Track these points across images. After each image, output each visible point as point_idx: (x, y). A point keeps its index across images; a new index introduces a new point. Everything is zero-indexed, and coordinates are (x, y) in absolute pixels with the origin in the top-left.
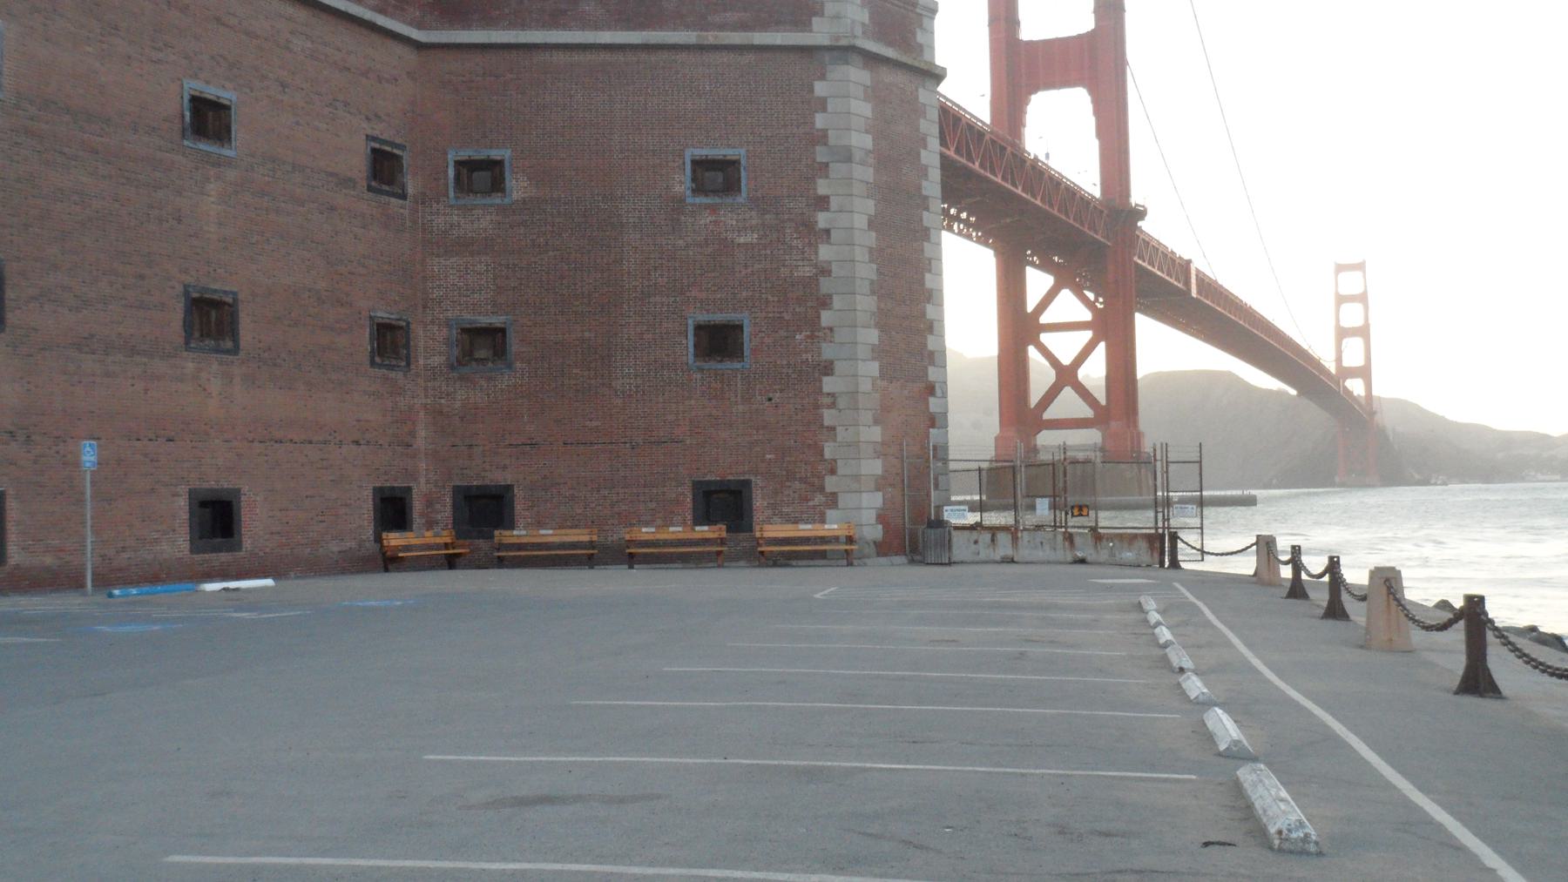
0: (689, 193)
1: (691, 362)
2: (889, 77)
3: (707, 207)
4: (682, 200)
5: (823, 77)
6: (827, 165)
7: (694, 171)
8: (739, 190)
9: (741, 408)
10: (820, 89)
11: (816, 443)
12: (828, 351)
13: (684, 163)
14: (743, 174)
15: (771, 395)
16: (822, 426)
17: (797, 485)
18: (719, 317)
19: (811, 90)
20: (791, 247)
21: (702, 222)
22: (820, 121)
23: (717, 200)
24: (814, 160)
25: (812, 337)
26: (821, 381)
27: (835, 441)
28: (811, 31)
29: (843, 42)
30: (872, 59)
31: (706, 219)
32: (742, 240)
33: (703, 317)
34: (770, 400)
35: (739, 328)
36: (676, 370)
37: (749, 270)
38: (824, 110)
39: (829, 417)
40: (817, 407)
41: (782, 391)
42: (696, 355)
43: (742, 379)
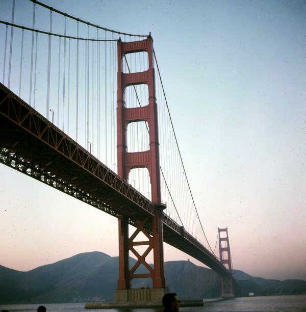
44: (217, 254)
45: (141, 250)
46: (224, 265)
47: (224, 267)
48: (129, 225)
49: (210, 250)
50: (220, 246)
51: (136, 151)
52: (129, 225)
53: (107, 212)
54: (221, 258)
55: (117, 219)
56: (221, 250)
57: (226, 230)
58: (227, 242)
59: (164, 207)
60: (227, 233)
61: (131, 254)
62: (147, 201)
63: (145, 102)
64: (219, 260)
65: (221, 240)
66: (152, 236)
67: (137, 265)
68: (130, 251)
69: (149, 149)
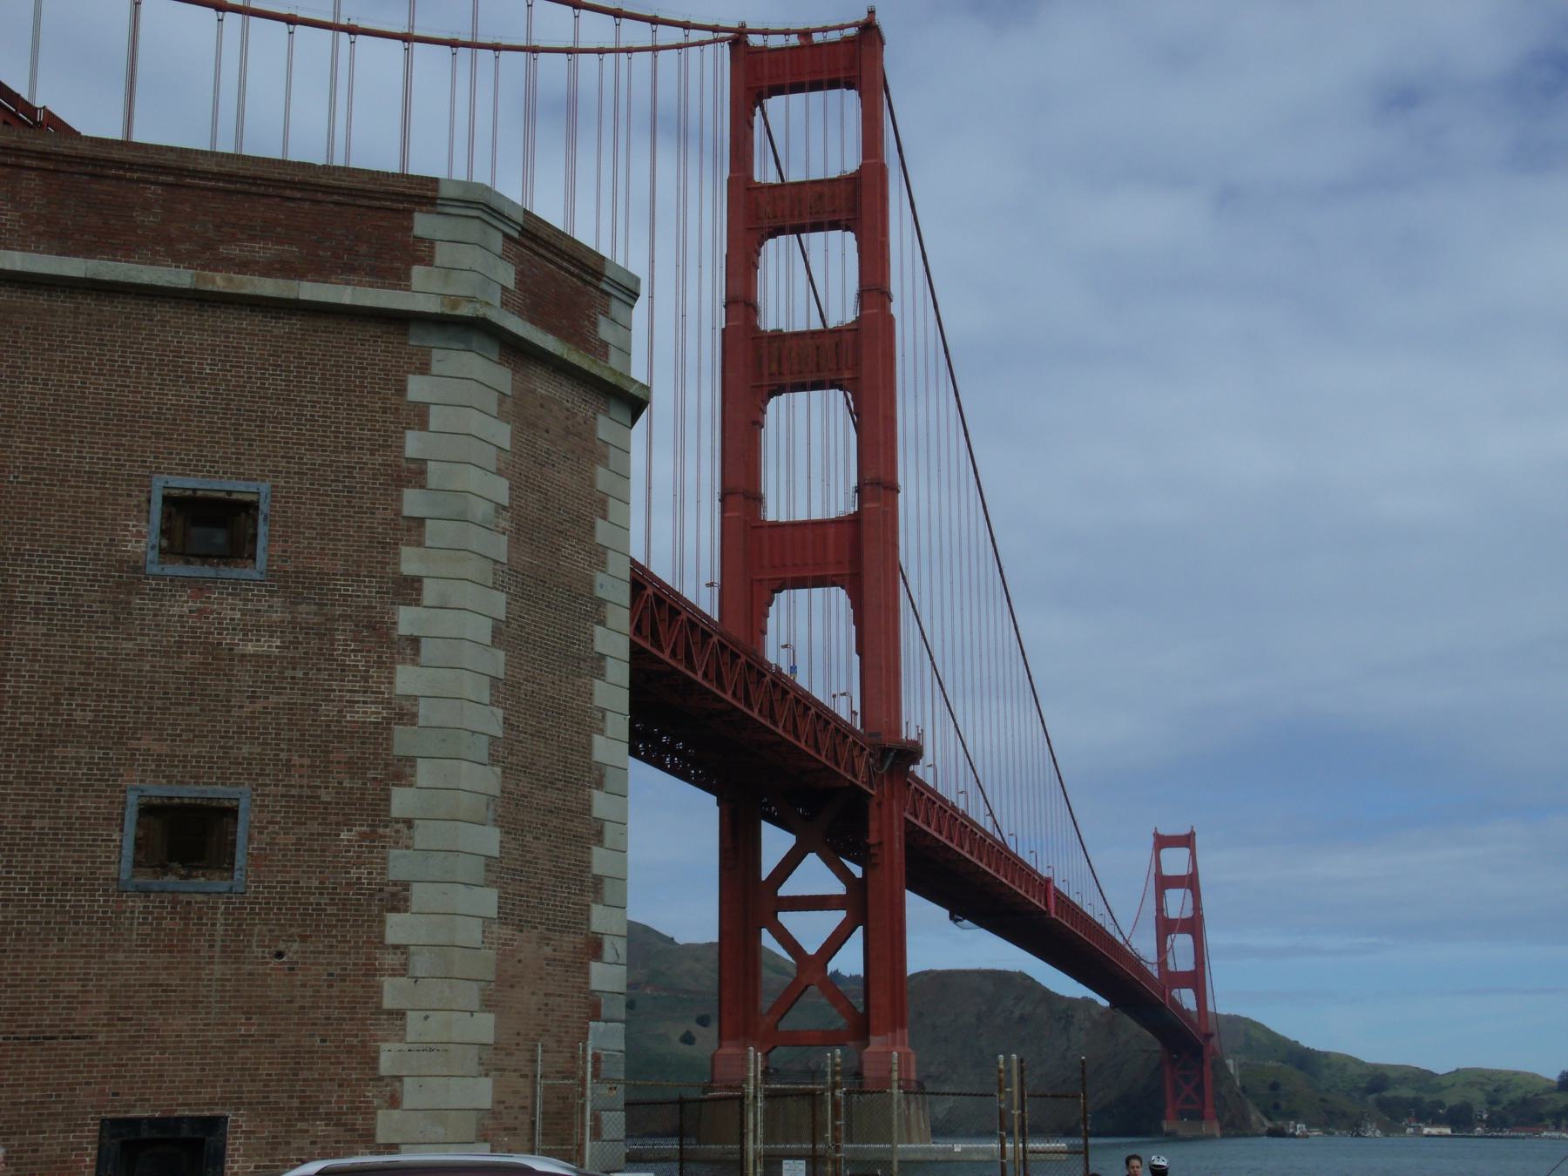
0: (153, 555)
1: (125, 876)
2: (544, 386)
3: (187, 582)
4: (137, 568)
5: (424, 369)
6: (420, 521)
7: (167, 517)
8: (253, 557)
9: (218, 970)
10: (418, 388)
11: (364, 1044)
12: (399, 865)
13: (149, 501)
14: (262, 529)
15: (281, 946)
16: (379, 1010)
17: (320, 1127)
18: (190, 792)
19: (402, 390)
20: (344, 668)
21: (176, 610)
22: (414, 444)
23: (208, 571)
24: (398, 513)
25: (371, 836)
26: (382, 922)
27: (402, 1040)
28: (408, 288)
29: (465, 310)
30: (515, 350)
31: (182, 605)
32: (250, 648)
33: (159, 790)
34: (280, 955)
35: (232, 812)
36: (92, 891)
37: (259, 706)
38: (423, 425)
39: (392, 992)
40: (371, 971)
41: (304, 938)
42: (137, 864)
43: (226, 913)
44: (1144, 945)
45: (811, 929)
46: (1175, 992)
47: (1177, 1006)
48: (764, 823)
49: (1110, 929)
50: (1160, 909)
51: (801, 516)
52: (764, 823)
53: (673, 772)
54: (1162, 963)
55: (714, 799)
56: (1165, 927)
57: (1187, 841)
58: (1188, 891)
59: (912, 753)
60: (1193, 855)
61: (768, 940)
62: (840, 730)
63: (842, 310)
64: (1154, 971)
65: (1164, 883)
66: (857, 871)
67: (791, 997)
68: (765, 931)
69: (853, 509)
